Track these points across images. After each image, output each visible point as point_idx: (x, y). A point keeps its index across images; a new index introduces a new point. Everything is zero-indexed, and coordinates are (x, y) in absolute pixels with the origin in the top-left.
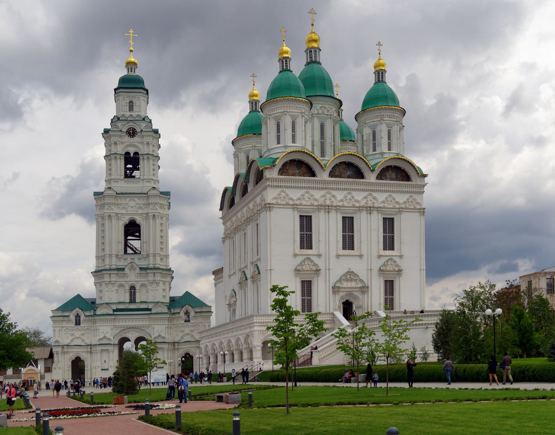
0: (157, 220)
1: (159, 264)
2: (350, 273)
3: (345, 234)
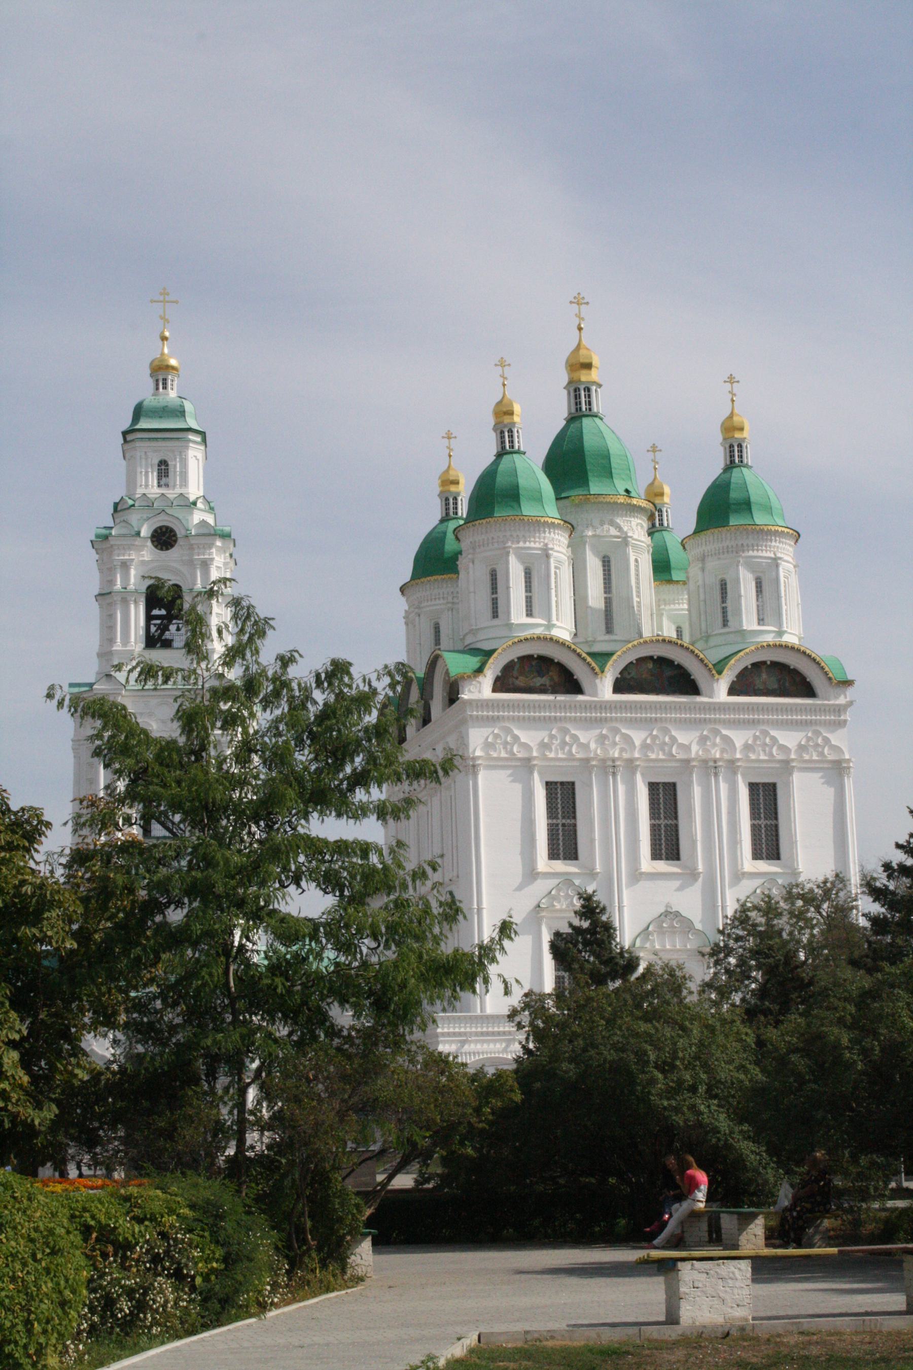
2: (670, 914)
3: (657, 822)
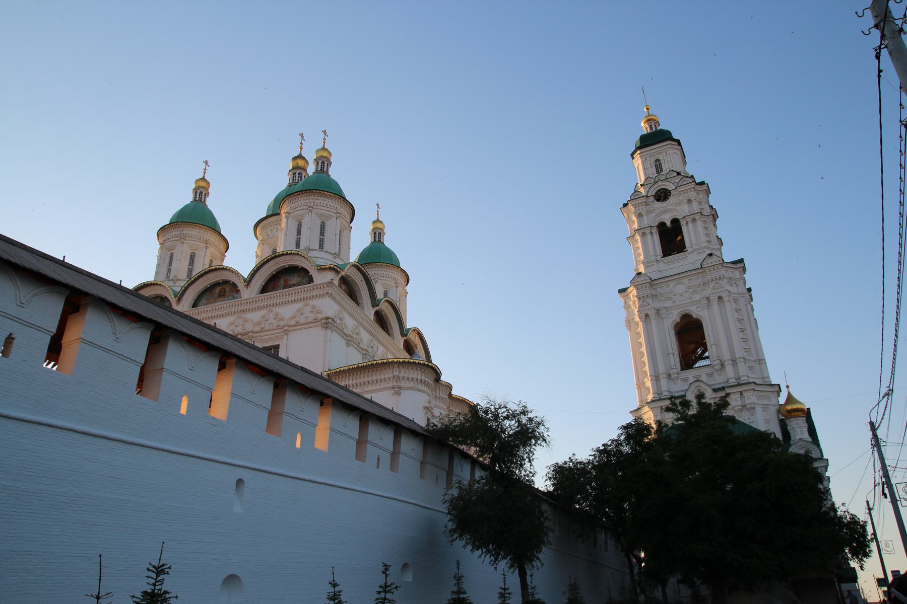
0: (727, 304)
1: (744, 371)
